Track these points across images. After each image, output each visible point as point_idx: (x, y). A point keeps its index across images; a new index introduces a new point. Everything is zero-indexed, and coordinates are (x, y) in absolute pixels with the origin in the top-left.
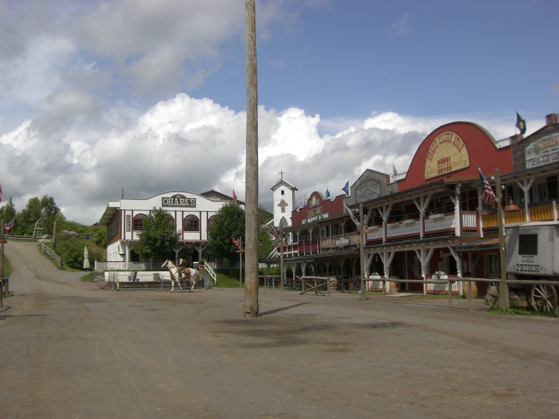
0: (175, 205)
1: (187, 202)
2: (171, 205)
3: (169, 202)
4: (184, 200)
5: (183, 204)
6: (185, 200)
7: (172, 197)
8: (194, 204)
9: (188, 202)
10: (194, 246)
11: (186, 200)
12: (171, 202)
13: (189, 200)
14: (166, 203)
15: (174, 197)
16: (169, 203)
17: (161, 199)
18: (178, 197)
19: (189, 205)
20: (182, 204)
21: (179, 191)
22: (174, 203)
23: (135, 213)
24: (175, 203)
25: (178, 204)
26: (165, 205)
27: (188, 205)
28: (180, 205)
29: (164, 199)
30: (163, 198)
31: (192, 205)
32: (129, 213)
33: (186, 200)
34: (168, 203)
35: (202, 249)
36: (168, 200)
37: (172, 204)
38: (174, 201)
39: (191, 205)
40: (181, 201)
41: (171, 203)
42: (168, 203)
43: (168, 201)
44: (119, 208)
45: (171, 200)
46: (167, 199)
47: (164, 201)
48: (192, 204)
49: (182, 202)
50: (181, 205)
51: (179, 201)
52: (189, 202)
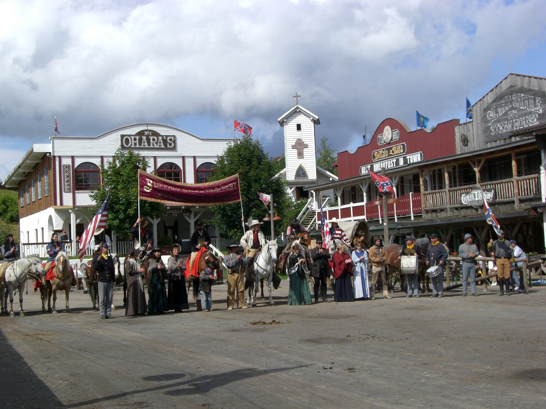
0: (142, 146)
1: (161, 141)
2: (135, 148)
3: (133, 142)
4: (156, 138)
6: (158, 139)
7: (137, 134)
8: (173, 145)
9: (163, 143)
10: (181, 212)
11: (160, 138)
12: (135, 142)
13: (165, 138)
14: (127, 144)
15: (141, 133)
16: (133, 143)
17: (120, 138)
18: (146, 133)
19: (164, 147)
20: (153, 145)
21: (147, 125)
22: (140, 144)
23: (78, 162)
24: (143, 144)
25: (147, 146)
26: (126, 148)
27: (163, 146)
29: (125, 138)
30: (122, 136)
31: (170, 147)
32: (67, 162)
33: (160, 138)
34: (130, 143)
35: (195, 218)
36: (131, 138)
38: (140, 140)
39: (168, 146)
40: (151, 141)
41: (135, 144)
42: (131, 145)
43: (130, 140)
44: (50, 153)
45: (135, 139)
47: (124, 141)
48: (170, 145)
49: (154, 142)
50: (152, 146)
51: (148, 140)
52: (165, 141)
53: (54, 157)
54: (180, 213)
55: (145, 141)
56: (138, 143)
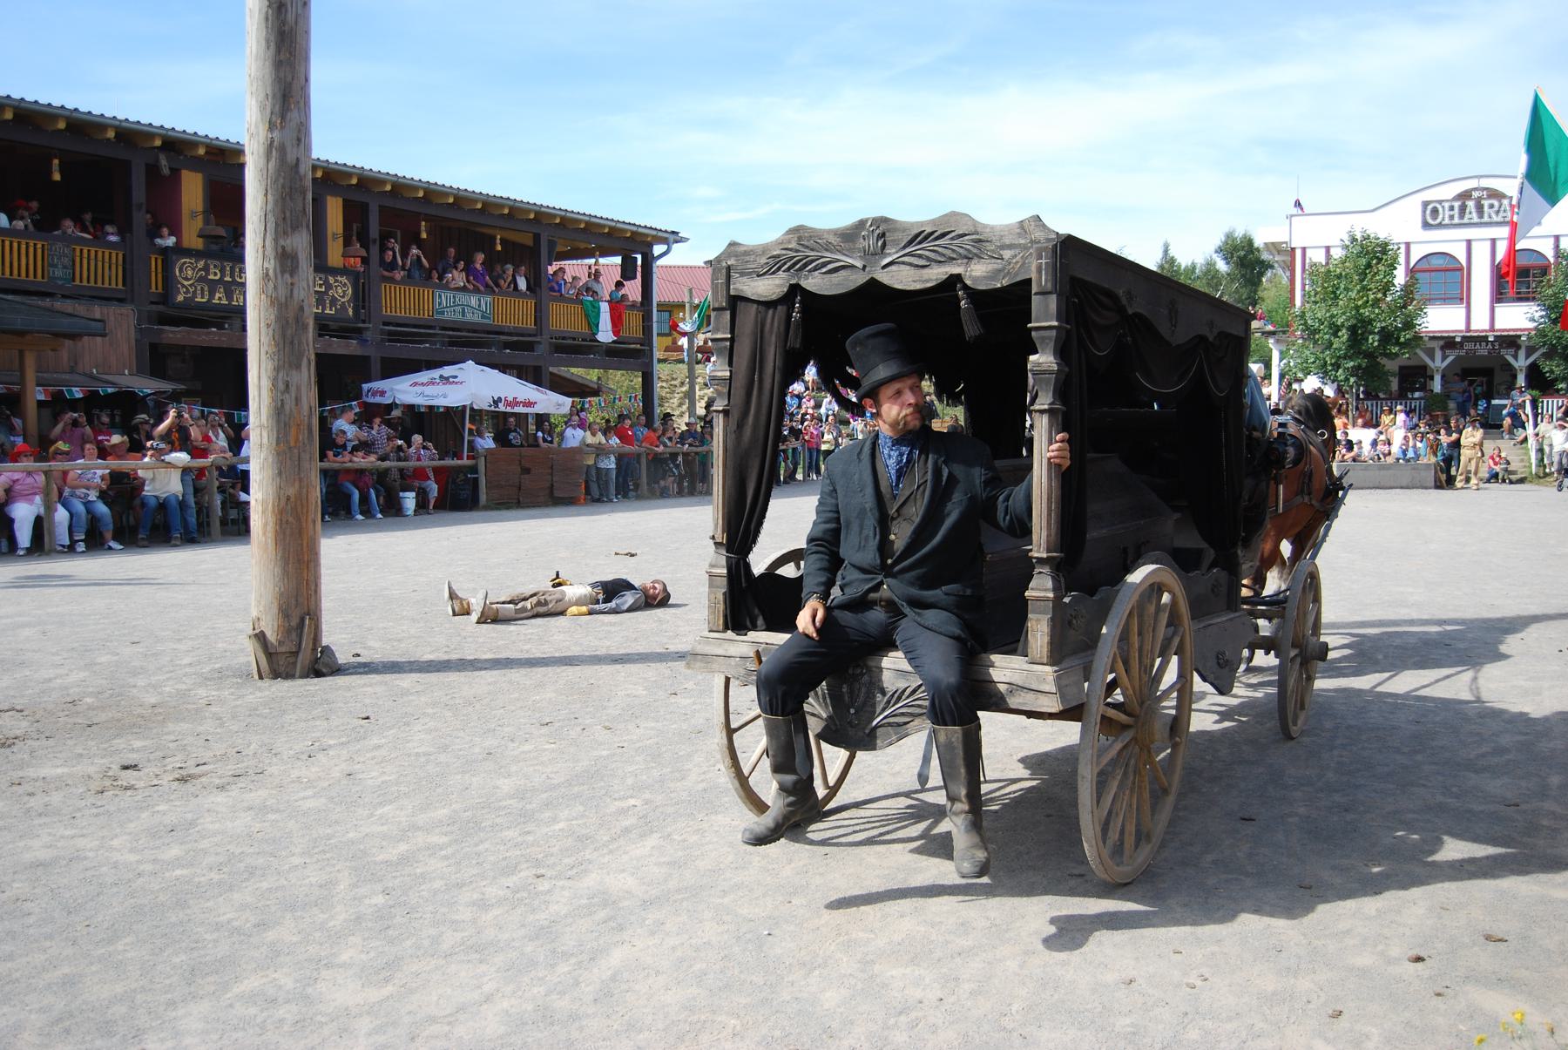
0: (1466, 221)
3: (1447, 213)
4: (1496, 203)
5: (1494, 215)
7: (1455, 199)
12: (1452, 213)
15: (1465, 196)
16: (1447, 216)
18: (1476, 194)
20: (1490, 217)
24: (1467, 216)
25: (1476, 219)
26: (1432, 225)
28: (1483, 220)
29: (1430, 207)
30: (1425, 204)
32: (1318, 256)
33: (1506, 202)
34: (1441, 216)
37: (1456, 220)
38: (1463, 209)
41: (1452, 217)
44: (1286, 243)
45: (1452, 208)
46: (1438, 206)
47: (1428, 212)
49: (1491, 211)
50: (1486, 219)
51: (1480, 208)
53: (1293, 249)
54: (1493, 349)
55: (1473, 210)
56: (1456, 216)
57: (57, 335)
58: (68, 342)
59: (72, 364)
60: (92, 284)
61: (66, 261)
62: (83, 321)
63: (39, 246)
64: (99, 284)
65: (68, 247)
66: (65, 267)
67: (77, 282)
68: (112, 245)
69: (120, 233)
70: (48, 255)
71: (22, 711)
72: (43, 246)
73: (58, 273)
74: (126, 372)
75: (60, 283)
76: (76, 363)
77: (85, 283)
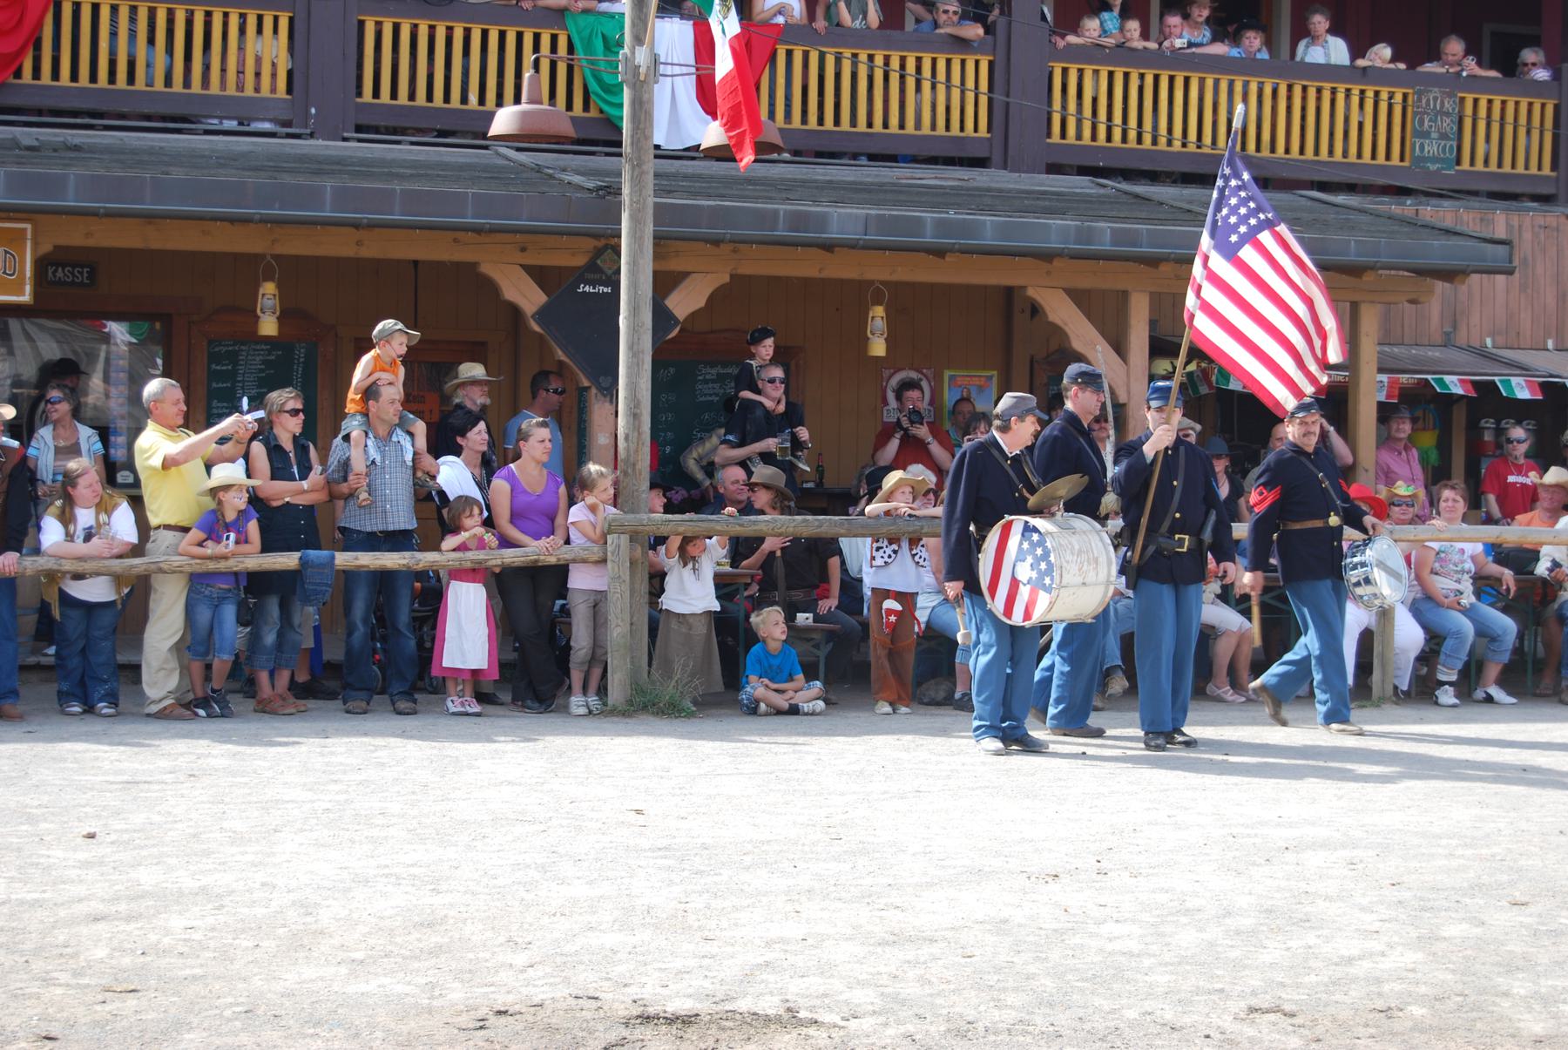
57: (1421, 272)
58: (1440, 286)
59: (1448, 329)
60: (1493, 167)
61: (1447, 124)
62: (1470, 243)
63: (1398, 98)
64: (1507, 168)
65: (1451, 95)
66: (1444, 136)
67: (1465, 166)
68: (1537, 89)
69: (1550, 63)
70: (1415, 114)
71: (1293, 1015)
72: (1405, 96)
73: (1432, 148)
74: (1550, 344)
75: (1433, 167)
76: (1455, 327)
77: (1479, 166)
